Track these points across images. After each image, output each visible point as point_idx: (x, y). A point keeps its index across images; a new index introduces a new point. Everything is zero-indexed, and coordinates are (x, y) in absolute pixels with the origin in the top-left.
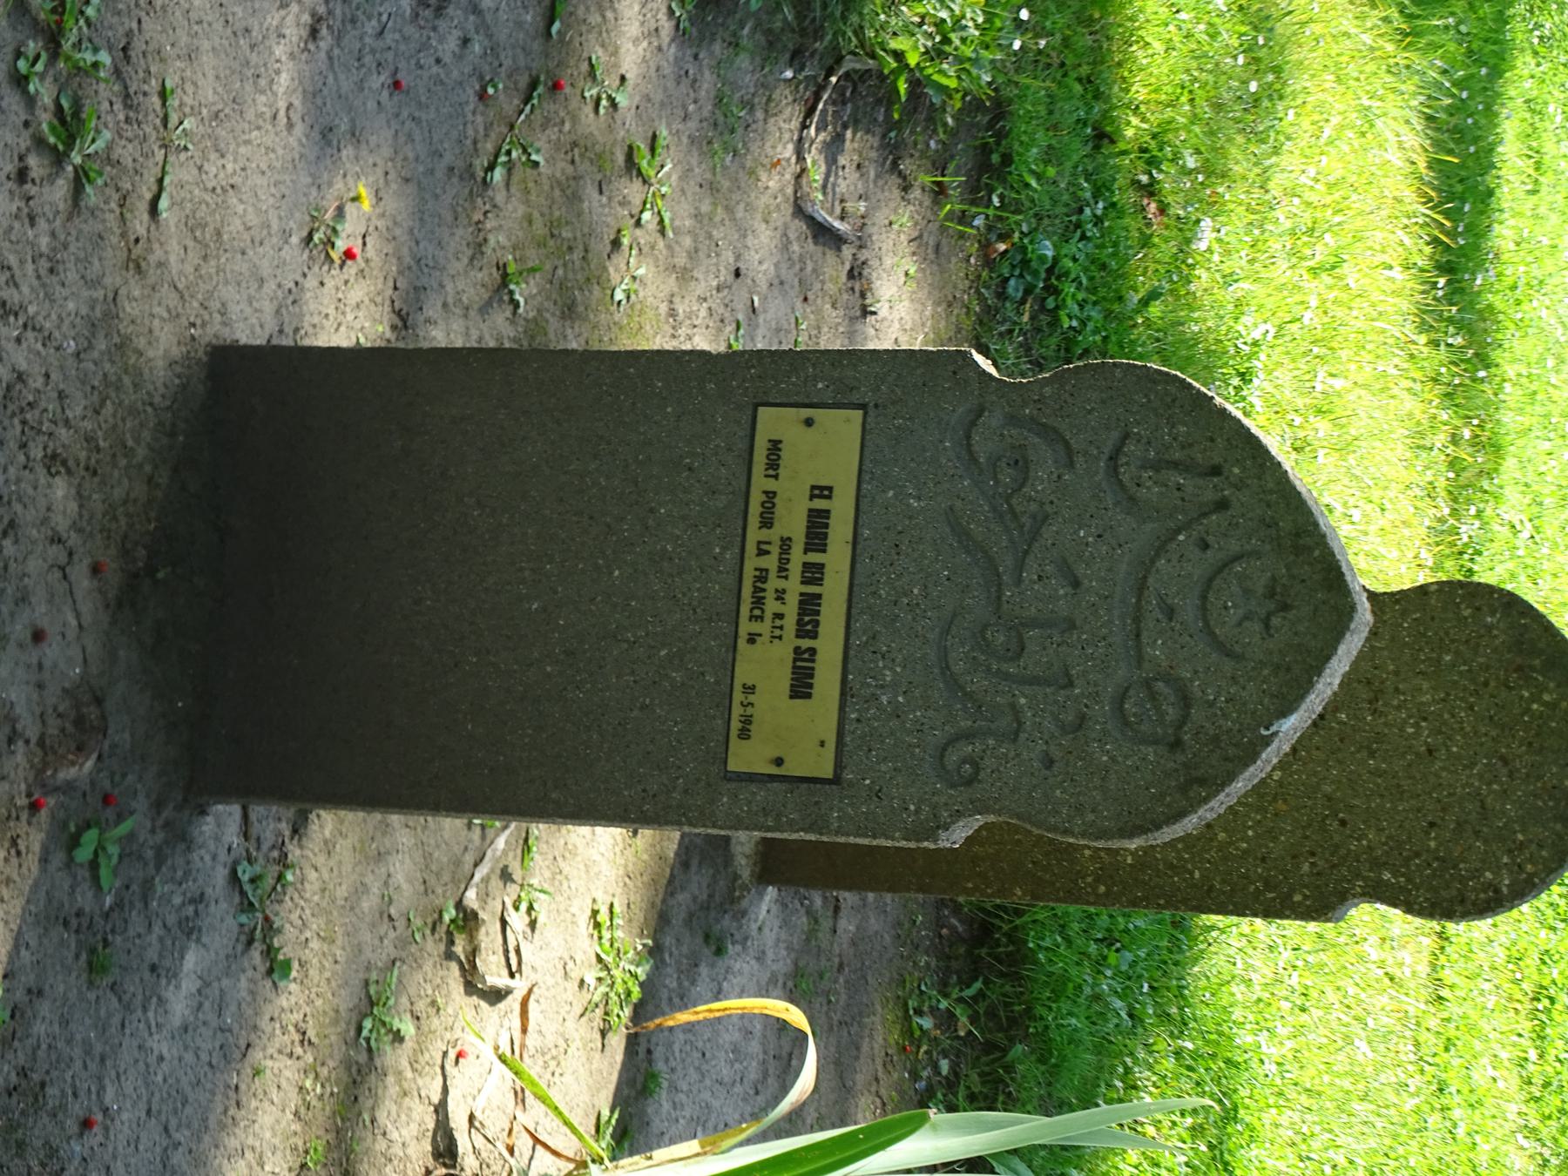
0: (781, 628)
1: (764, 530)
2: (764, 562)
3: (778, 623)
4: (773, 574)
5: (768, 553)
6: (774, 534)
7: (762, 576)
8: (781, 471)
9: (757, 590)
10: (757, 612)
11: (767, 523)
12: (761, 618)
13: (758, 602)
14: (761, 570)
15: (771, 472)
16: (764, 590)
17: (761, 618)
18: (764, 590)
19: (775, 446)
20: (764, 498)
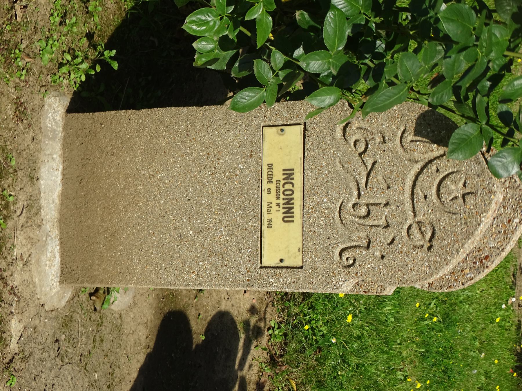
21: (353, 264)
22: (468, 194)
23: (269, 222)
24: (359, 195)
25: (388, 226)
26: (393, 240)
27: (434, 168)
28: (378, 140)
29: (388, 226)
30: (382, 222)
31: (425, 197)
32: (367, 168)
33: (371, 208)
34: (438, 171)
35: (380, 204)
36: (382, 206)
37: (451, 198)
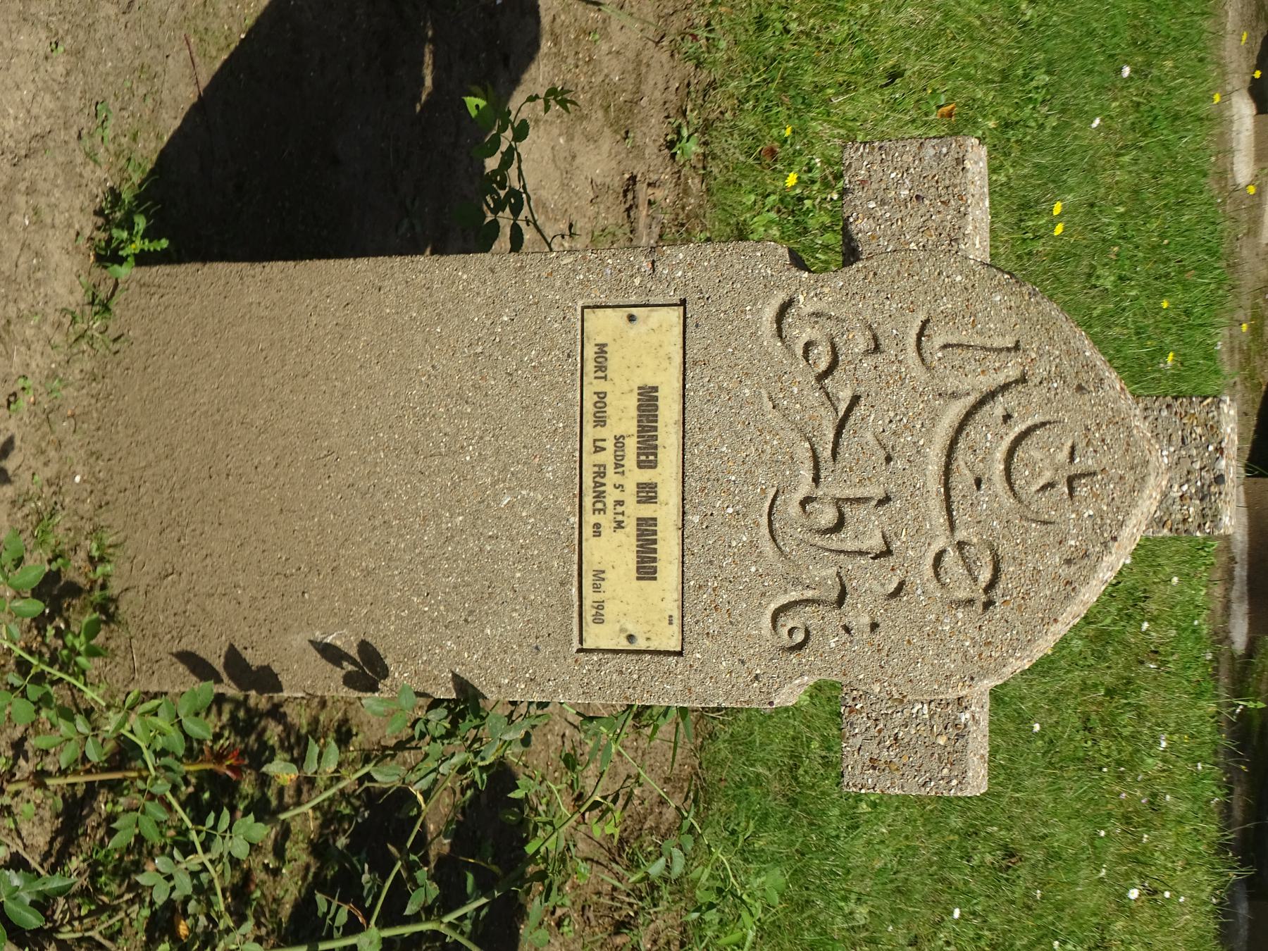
0: (623, 514)
1: (599, 427)
2: (601, 458)
3: (619, 509)
4: (610, 470)
5: (604, 449)
6: (608, 433)
7: (601, 472)
8: (610, 373)
9: (598, 485)
10: (599, 506)
11: (600, 421)
12: (603, 510)
13: (599, 496)
14: (599, 466)
15: (600, 374)
16: (604, 485)
17: (603, 510)
18: (604, 485)
19: (602, 349)
20: (596, 398)
21: (800, 646)
22: (1083, 475)
23: (597, 608)
24: (816, 479)
25: (888, 552)
26: (901, 585)
27: (999, 411)
28: (861, 342)
29: (888, 552)
30: (876, 543)
31: (978, 482)
32: (836, 410)
33: (847, 509)
34: (1007, 417)
35: (870, 499)
36: (874, 503)
37: (1042, 482)
